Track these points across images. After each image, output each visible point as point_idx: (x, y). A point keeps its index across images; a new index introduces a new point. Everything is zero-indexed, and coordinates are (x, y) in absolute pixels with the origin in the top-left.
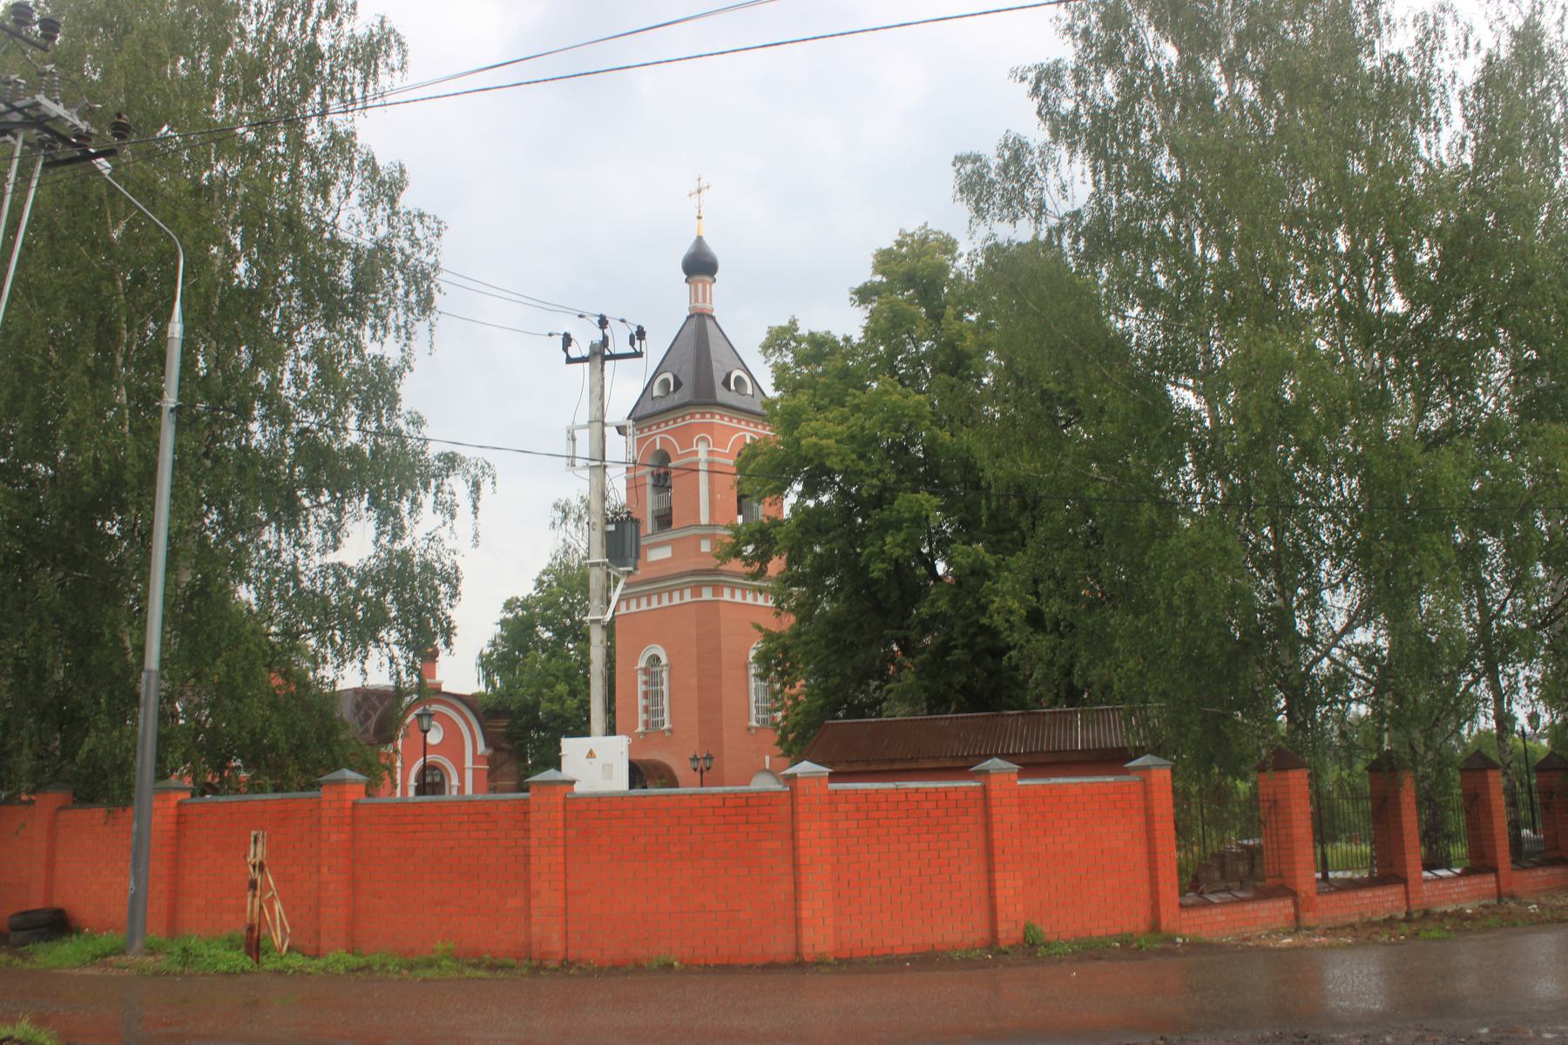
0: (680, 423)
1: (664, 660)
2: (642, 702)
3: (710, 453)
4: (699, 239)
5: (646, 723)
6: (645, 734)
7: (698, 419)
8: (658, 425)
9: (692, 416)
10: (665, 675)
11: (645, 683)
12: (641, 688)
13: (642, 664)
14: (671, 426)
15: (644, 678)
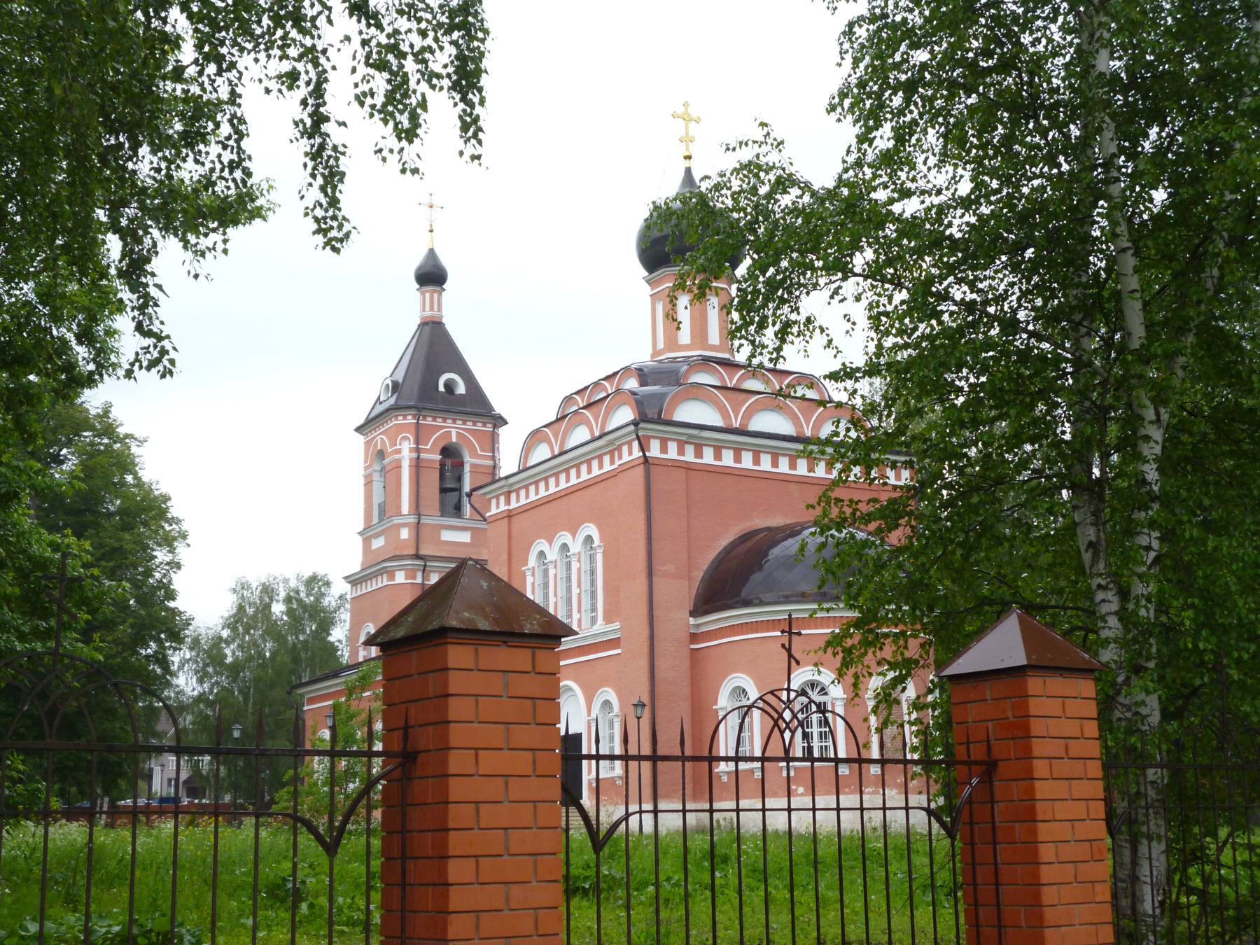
4: (432, 251)
8: (454, 421)
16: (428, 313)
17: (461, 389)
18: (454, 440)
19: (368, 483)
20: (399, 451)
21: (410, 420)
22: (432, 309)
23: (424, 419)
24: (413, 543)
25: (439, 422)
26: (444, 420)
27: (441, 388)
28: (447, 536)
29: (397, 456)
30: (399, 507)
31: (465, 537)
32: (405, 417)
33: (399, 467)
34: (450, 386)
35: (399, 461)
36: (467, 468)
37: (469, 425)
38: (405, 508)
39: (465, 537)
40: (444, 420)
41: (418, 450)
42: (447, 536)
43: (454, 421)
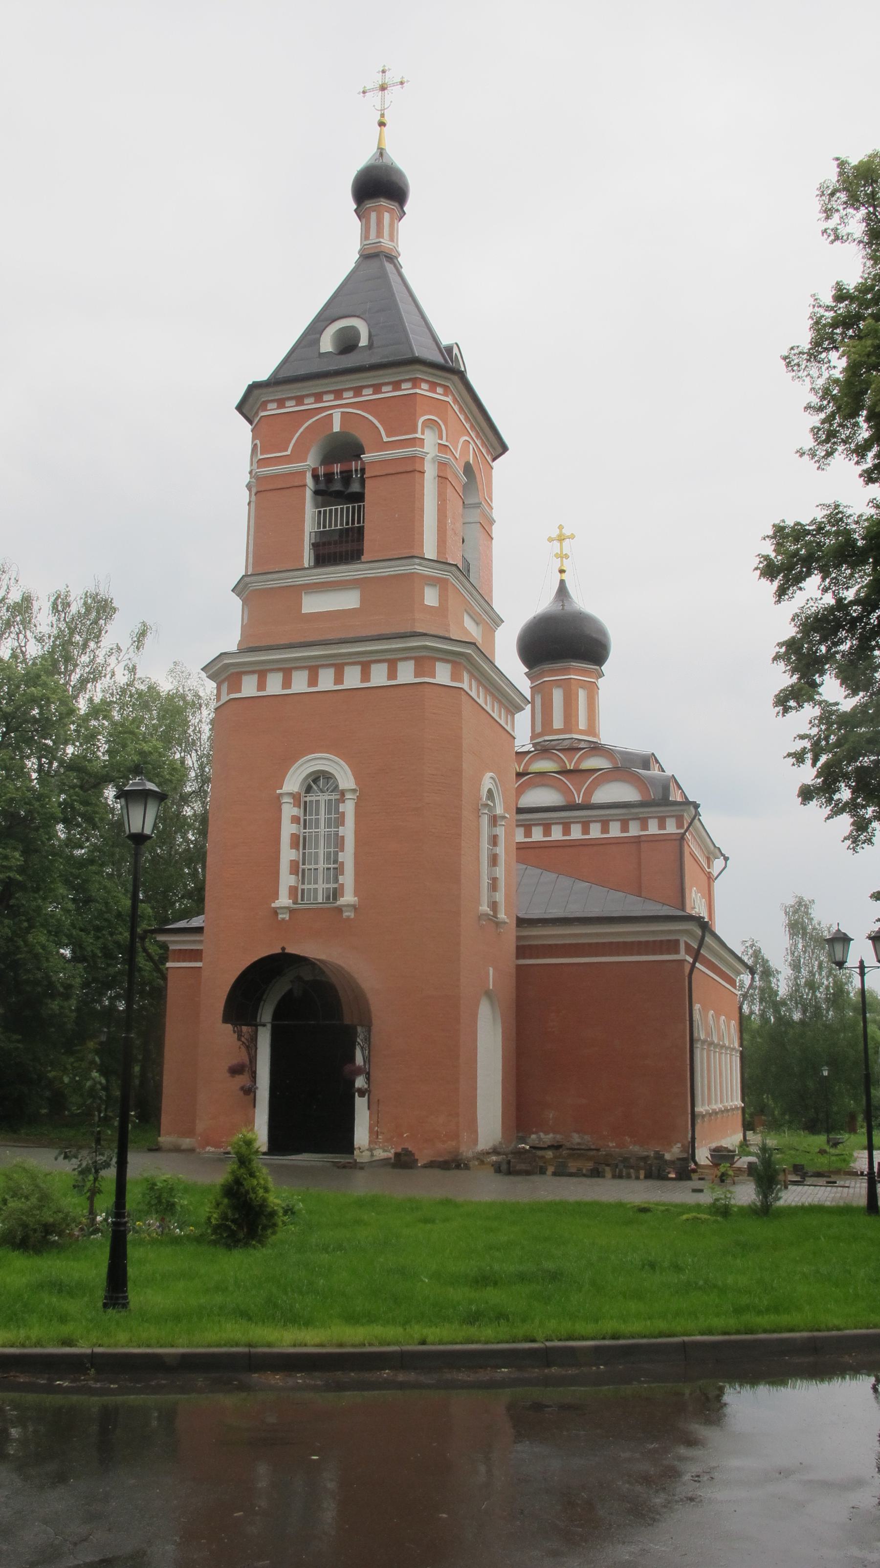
0: (387, 392)
1: (346, 780)
2: (287, 854)
3: (442, 447)
4: (381, 152)
5: (293, 891)
6: (291, 911)
7: (423, 390)
8: (338, 394)
9: (415, 382)
10: (348, 808)
11: (295, 820)
12: (288, 829)
13: (292, 783)
14: (368, 395)
15: (295, 811)
18: (336, 428)
25: (310, 404)
26: (318, 397)
28: (312, 604)
31: (349, 600)
37: (368, 395)
39: (349, 600)
40: (318, 397)
42: (312, 604)
43: (338, 394)
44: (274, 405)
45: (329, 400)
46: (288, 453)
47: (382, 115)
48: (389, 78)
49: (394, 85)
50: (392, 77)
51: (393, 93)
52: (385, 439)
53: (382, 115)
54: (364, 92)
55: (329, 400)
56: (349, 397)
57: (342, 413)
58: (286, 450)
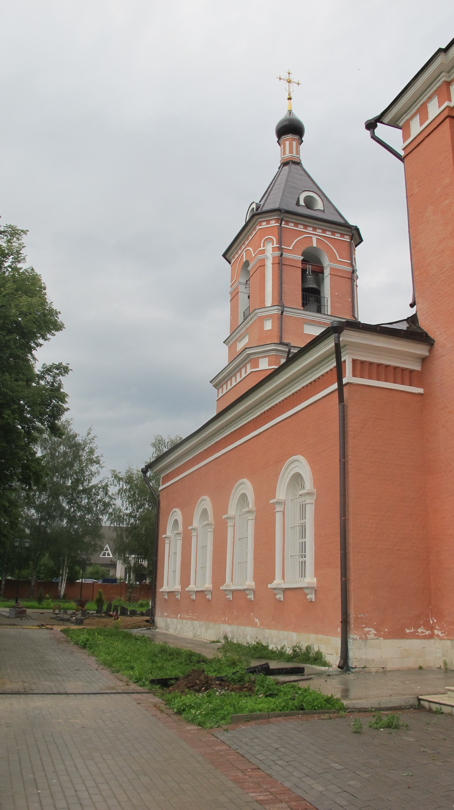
4: (290, 112)
8: (315, 229)
16: (288, 154)
17: (320, 205)
18: (315, 245)
19: (234, 296)
20: (263, 252)
21: (273, 223)
22: (291, 152)
23: (287, 223)
24: (276, 333)
25: (300, 228)
26: (306, 227)
27: (302, 203)
29: (261, 257)
30: (263, 300)
32: (268, 222)
33: (262, 266)
34: (309, 203)
35: (263, 260)
36: (327, 272)
37: (328, 234)
38: (269, 302)
41: (280, 249)
43: (315, 229)
44: (293, 225)
45: (310, 230)
46: (291, 248)
47: (289, 95)
48: (292, 77)
49: (295, 83)
50: (285, 76)
51: (293, 87)
52: (339, 259)
53: (289, 95)
54: (280, 79)
55: (310, 230)
56: (319, 232)
57: (317, 238)
58: (290, 247)
